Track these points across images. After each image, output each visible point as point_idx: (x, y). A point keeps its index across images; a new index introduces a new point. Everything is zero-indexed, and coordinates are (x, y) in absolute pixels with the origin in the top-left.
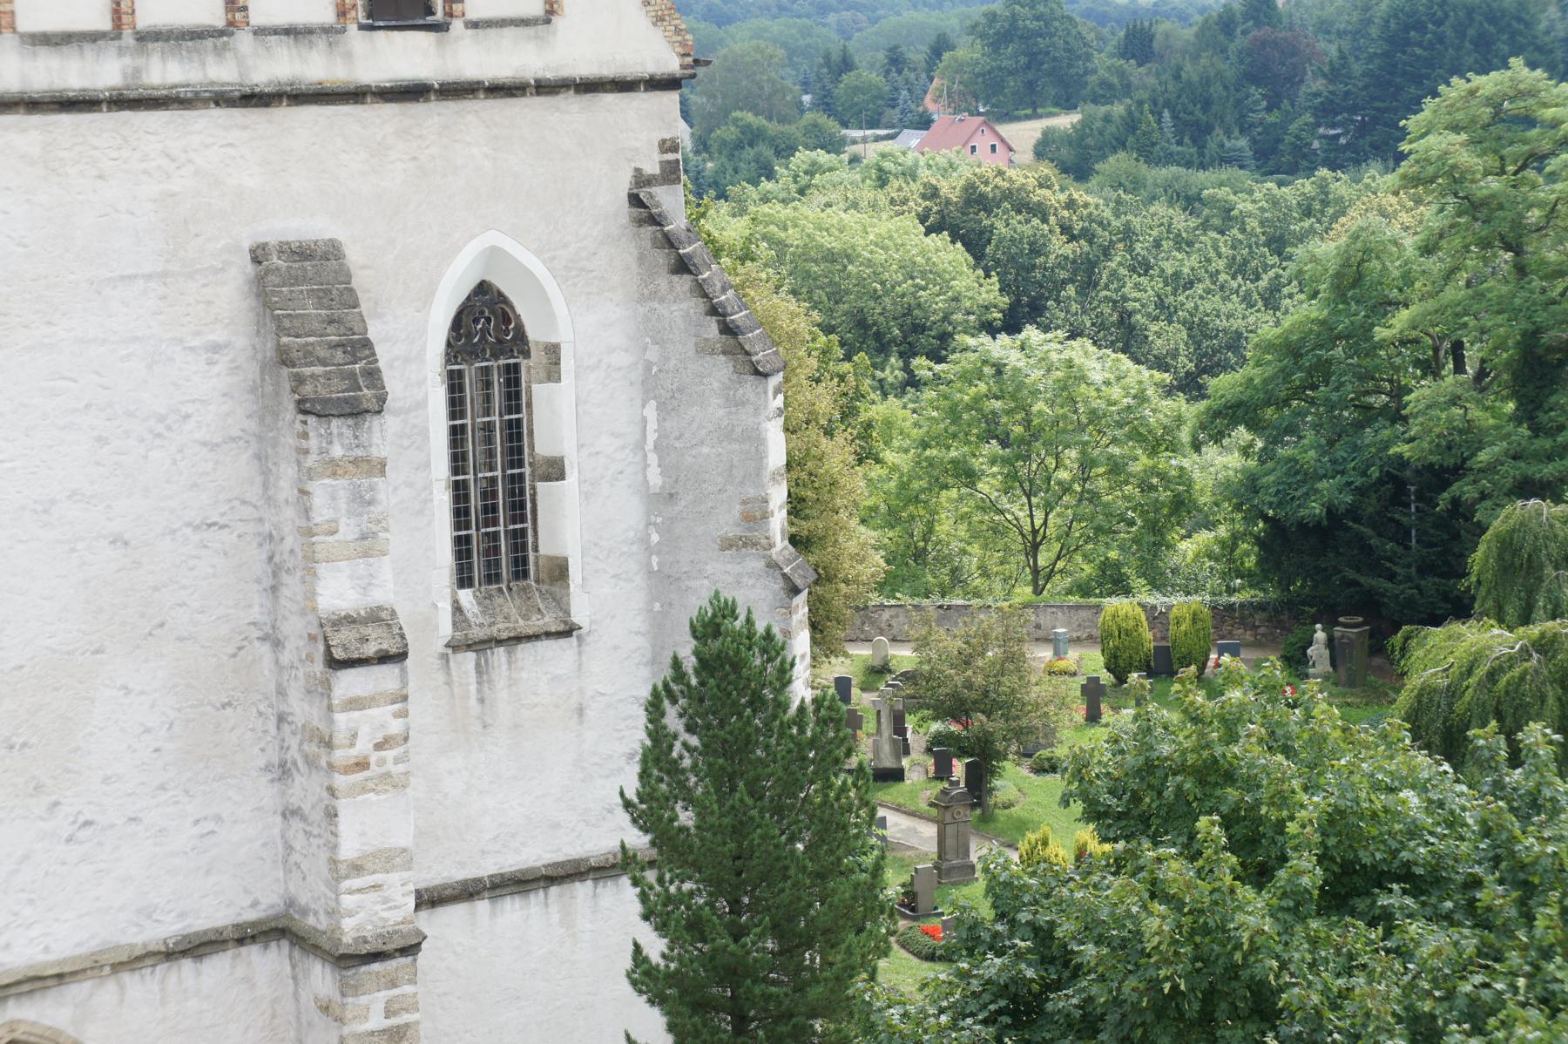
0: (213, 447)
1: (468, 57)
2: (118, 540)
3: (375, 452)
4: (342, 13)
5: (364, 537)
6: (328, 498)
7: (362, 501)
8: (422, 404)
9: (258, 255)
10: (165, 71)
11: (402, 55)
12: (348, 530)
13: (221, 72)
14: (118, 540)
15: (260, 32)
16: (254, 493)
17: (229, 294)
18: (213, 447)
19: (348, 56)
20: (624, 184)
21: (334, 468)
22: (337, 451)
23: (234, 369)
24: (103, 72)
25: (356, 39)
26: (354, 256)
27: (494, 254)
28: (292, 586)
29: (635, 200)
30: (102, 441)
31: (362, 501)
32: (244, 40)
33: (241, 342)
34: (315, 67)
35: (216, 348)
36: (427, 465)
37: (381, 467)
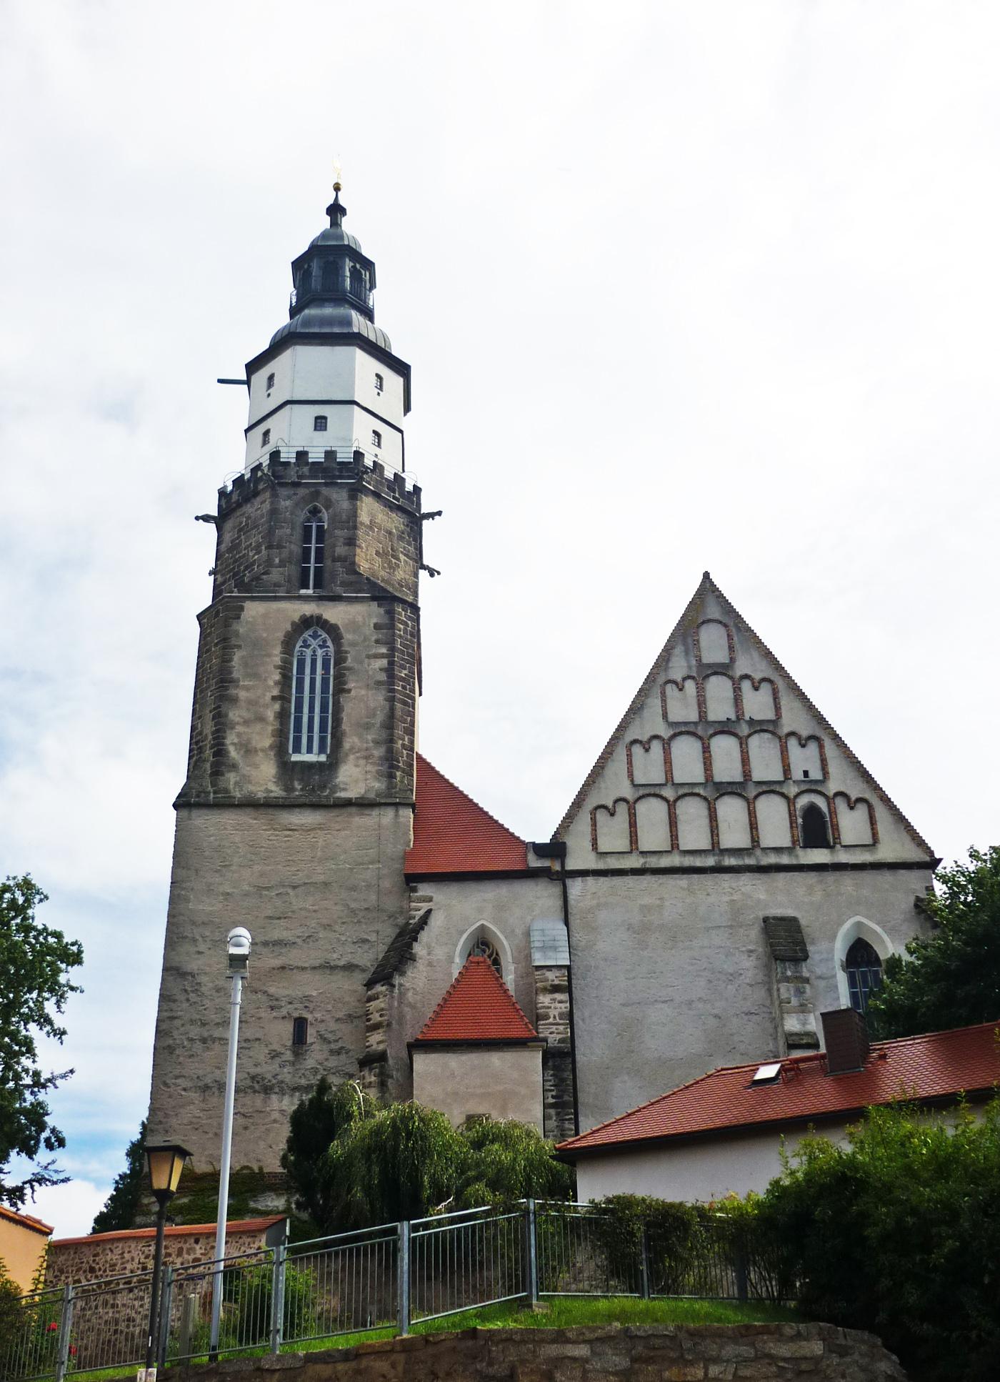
0: (751, 986)
1: (843, 857)
2: (716, 1016)
3: (806, 974)
4: (794, 842)
5: (801, 1005)
6: (786, 990)
7: (800, 992)
8: (834, 976)
9: (766, 920)
10: (730, 861)
11: (819, 856)
12: (795, 1002)
13: (750, 861)
14: (716, 1016)
15: (764, 849)
16: (768, 1003)
17: (755, 933)
18: (751, 986)
19: (797, 856)
20: (912, 900)
21: (787, 980)
22: (789, 973)
23: (758, 959)
24: (710, 861)
25: (800, 852)
26: (803, 922)
27: (859, 925)
28: (779, 1030)
29: (916, 906)
30: (710, 981)
31: (800, 992)
32: (758, 852)
33: (761, 950)
34: (785, 860)
35: (751, 951)
36: (838, 998)
37: (807, 981)
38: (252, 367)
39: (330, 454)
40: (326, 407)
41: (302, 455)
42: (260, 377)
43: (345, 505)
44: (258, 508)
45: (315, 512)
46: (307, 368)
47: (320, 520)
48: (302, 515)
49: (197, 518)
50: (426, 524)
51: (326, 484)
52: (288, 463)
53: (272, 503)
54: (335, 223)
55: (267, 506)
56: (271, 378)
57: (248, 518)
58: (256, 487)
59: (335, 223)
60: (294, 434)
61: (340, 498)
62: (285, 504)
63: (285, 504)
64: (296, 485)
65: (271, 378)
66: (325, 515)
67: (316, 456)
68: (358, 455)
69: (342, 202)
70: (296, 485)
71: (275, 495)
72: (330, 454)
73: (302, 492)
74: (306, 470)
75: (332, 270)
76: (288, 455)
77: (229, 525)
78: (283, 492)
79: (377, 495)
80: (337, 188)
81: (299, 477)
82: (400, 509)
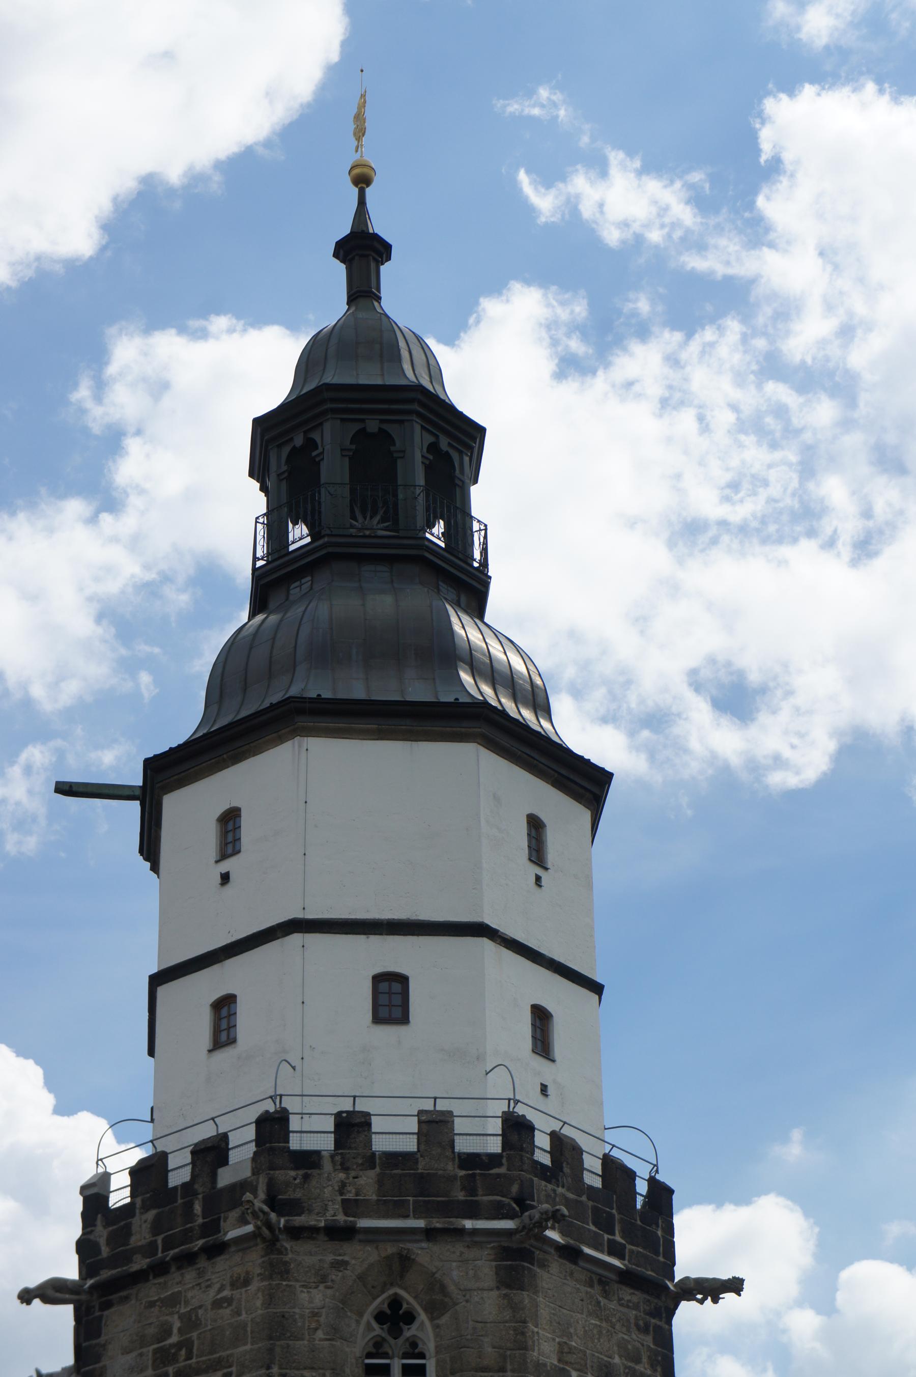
38: (166, 772)
39: (435, 1126)
40: (397, 952)
41: (351, 1126)
42: (190, 811)
43: (488, 1304)
44: (219, 1297)
45: (395, 1317)
46: (345, 811)
47: (414, 1349)
48: (363, 1331)
49: (26, 1296)
50: (688, 1317)
51: (430, 1234)
52: (308, 1160)
53: (270, 1299)
54: (363, 292)
55: (253, 1303)
56: (230, 820)
57: (191, 1322)
58: (212, 1227)
59: (363, 292)
60: (320, 1057)
61: (468, 1272)
62: (312, 1299)
63: (312, 1299)
64: (341, 1233)
65: (230, 820)
66: (424, 1330)
67: (394, 1132)
68: (517, 1128)
69: (379, 226)
70: (341, 1233)
71: (278, 1270)
72: (435, 1126)
73: (362, 1257)
74: (367, 1182)
75: (373, 462)
76: (312, 1132)
77: (122, 1322)
78: (305, 1256)
79: (570, 1254)
80: (362, 181)
81: (350, 1207)
82: (627, 1278)
